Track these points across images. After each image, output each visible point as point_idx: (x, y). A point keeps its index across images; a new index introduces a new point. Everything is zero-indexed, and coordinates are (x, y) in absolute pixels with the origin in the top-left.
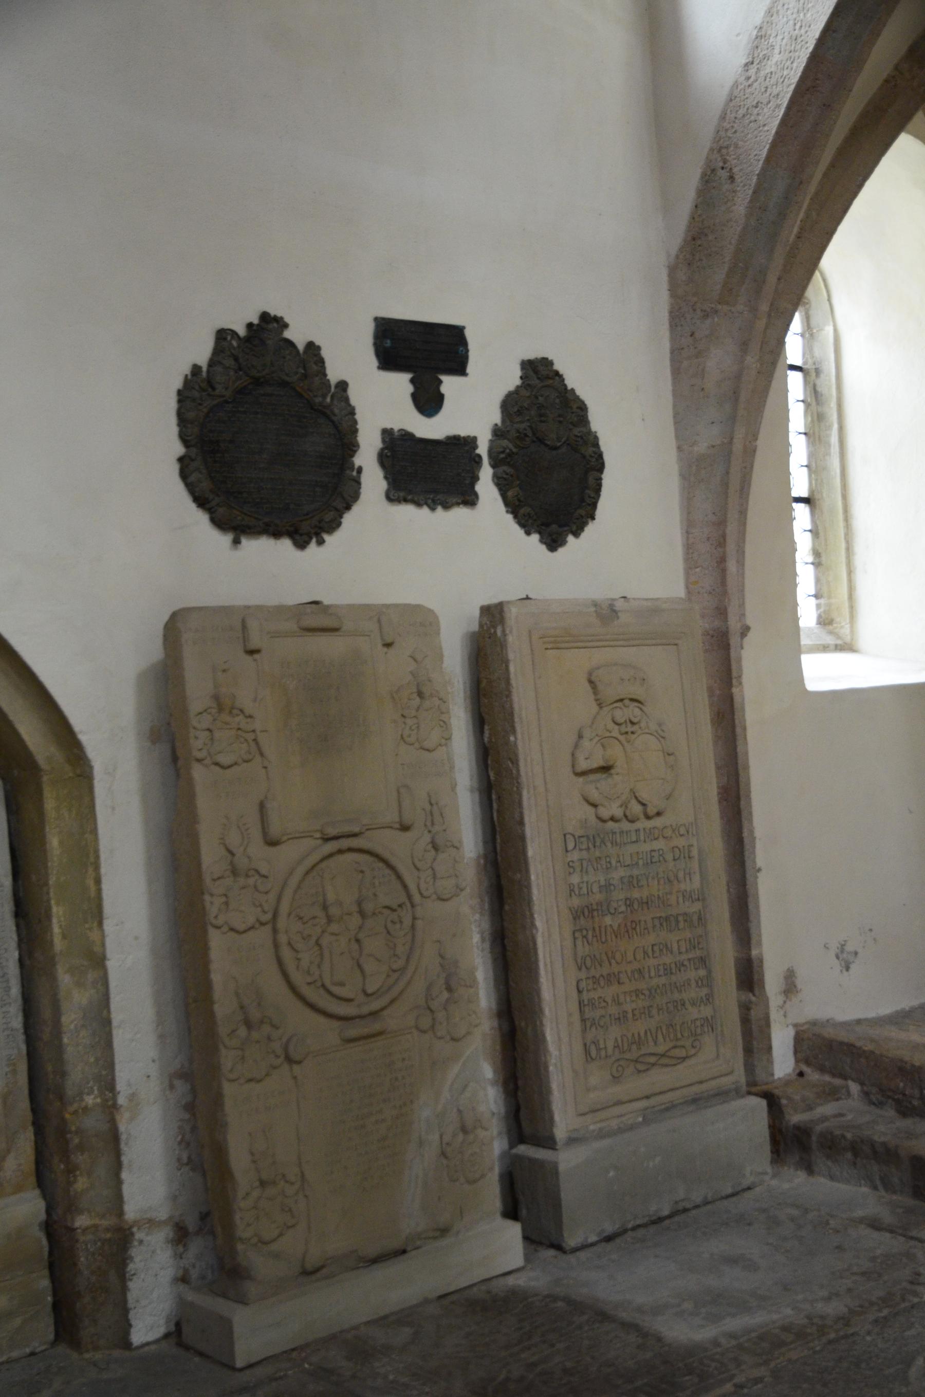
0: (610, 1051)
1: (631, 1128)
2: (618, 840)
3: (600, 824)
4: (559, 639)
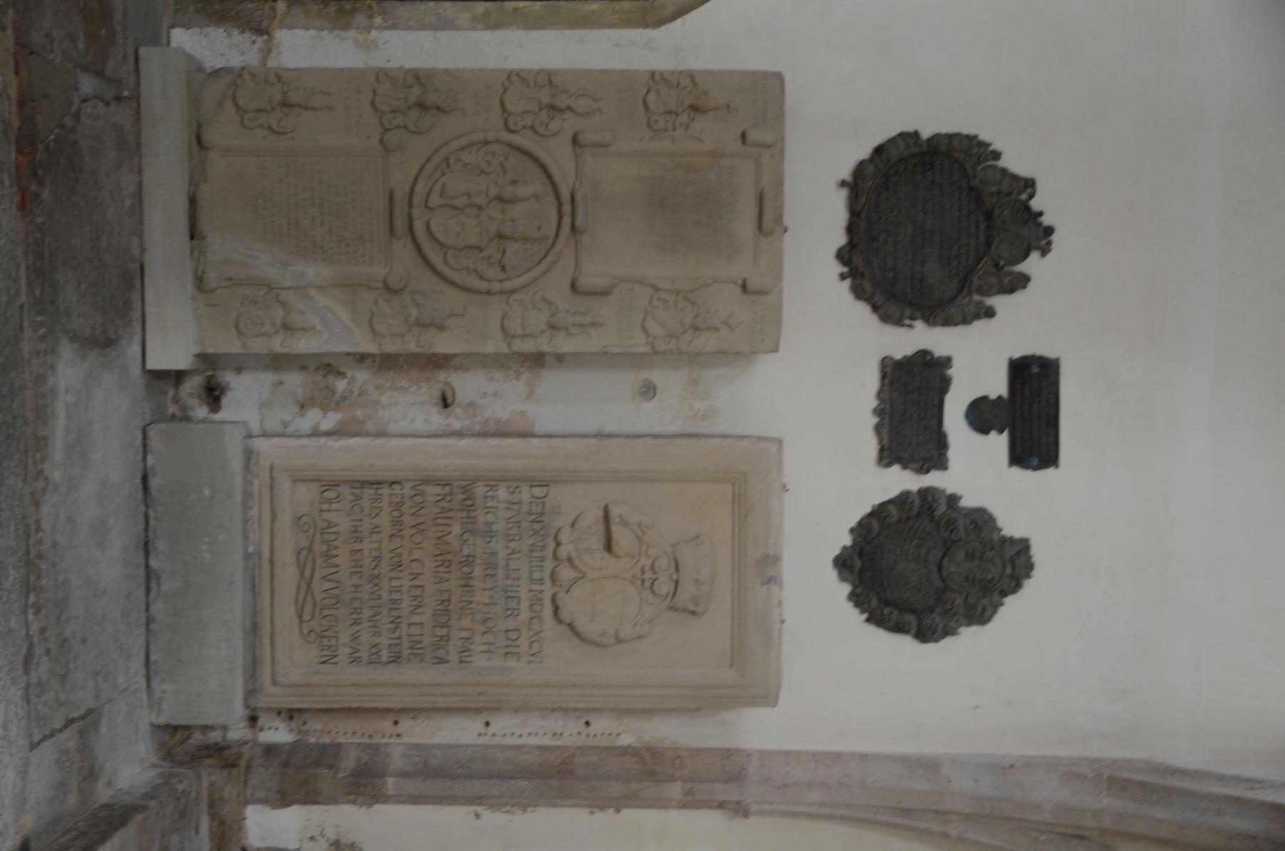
0: (326, 516)
1: (246, 537)
2: (535, 554)
3: (554, 531)
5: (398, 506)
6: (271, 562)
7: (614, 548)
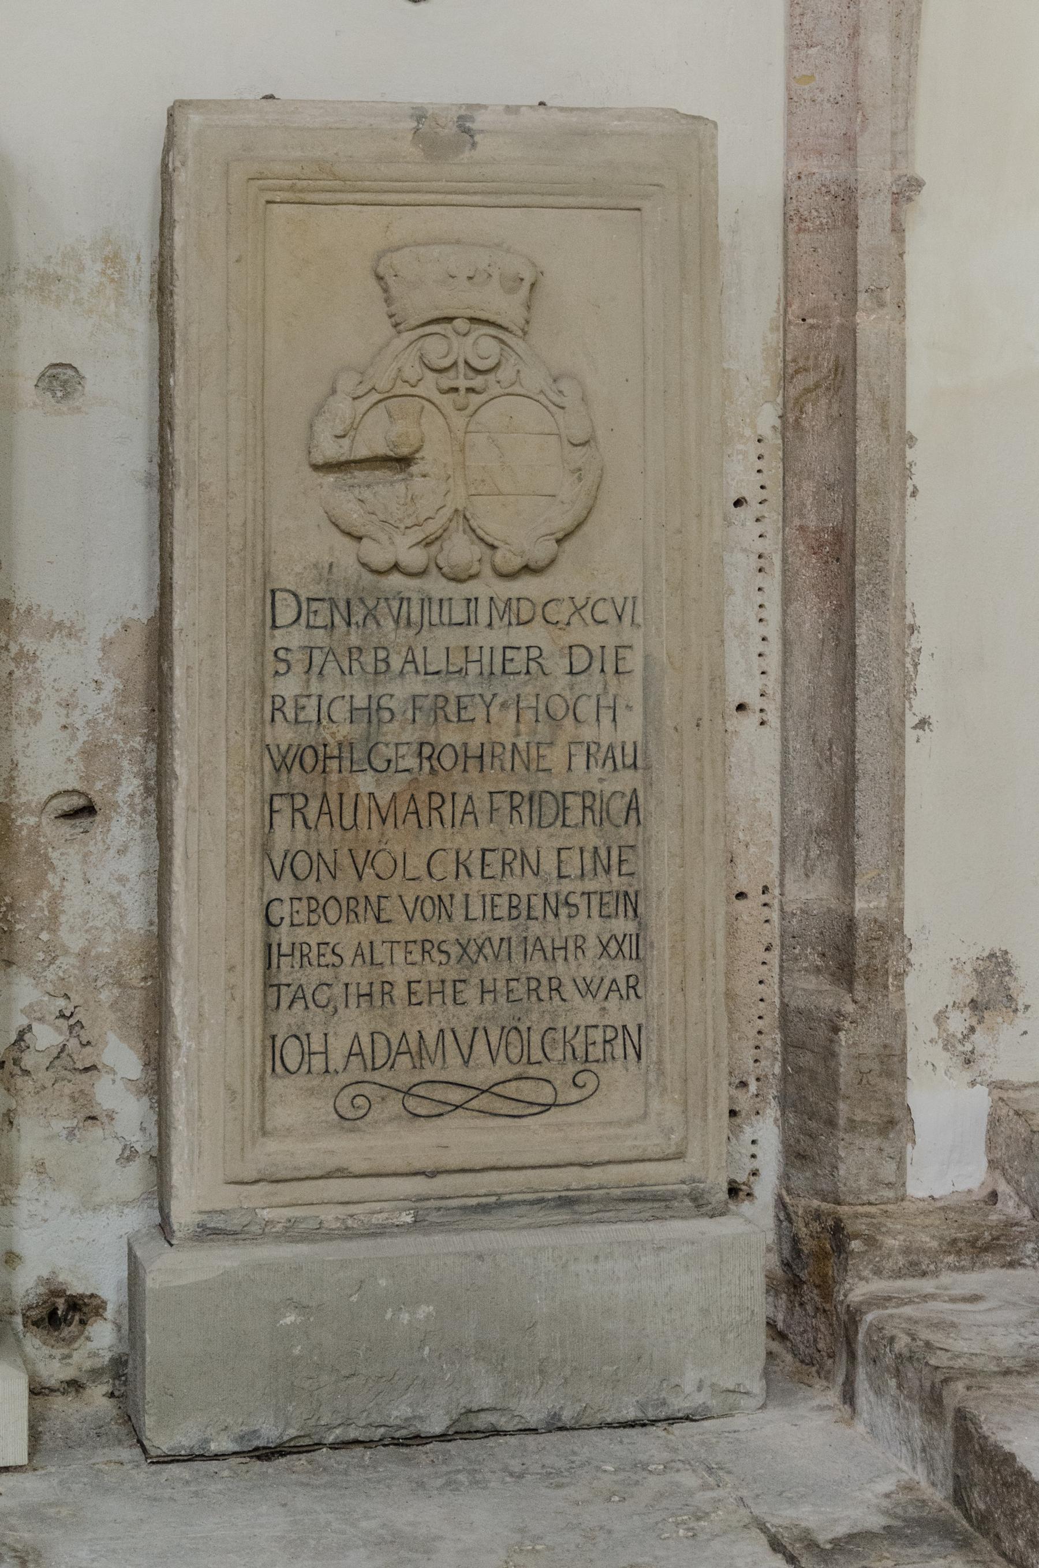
2: (415, 616)
3: (368, 577)
4: (300, 184)
5: (317, 907)
6: (433, 1174)
7: (404, 451)
